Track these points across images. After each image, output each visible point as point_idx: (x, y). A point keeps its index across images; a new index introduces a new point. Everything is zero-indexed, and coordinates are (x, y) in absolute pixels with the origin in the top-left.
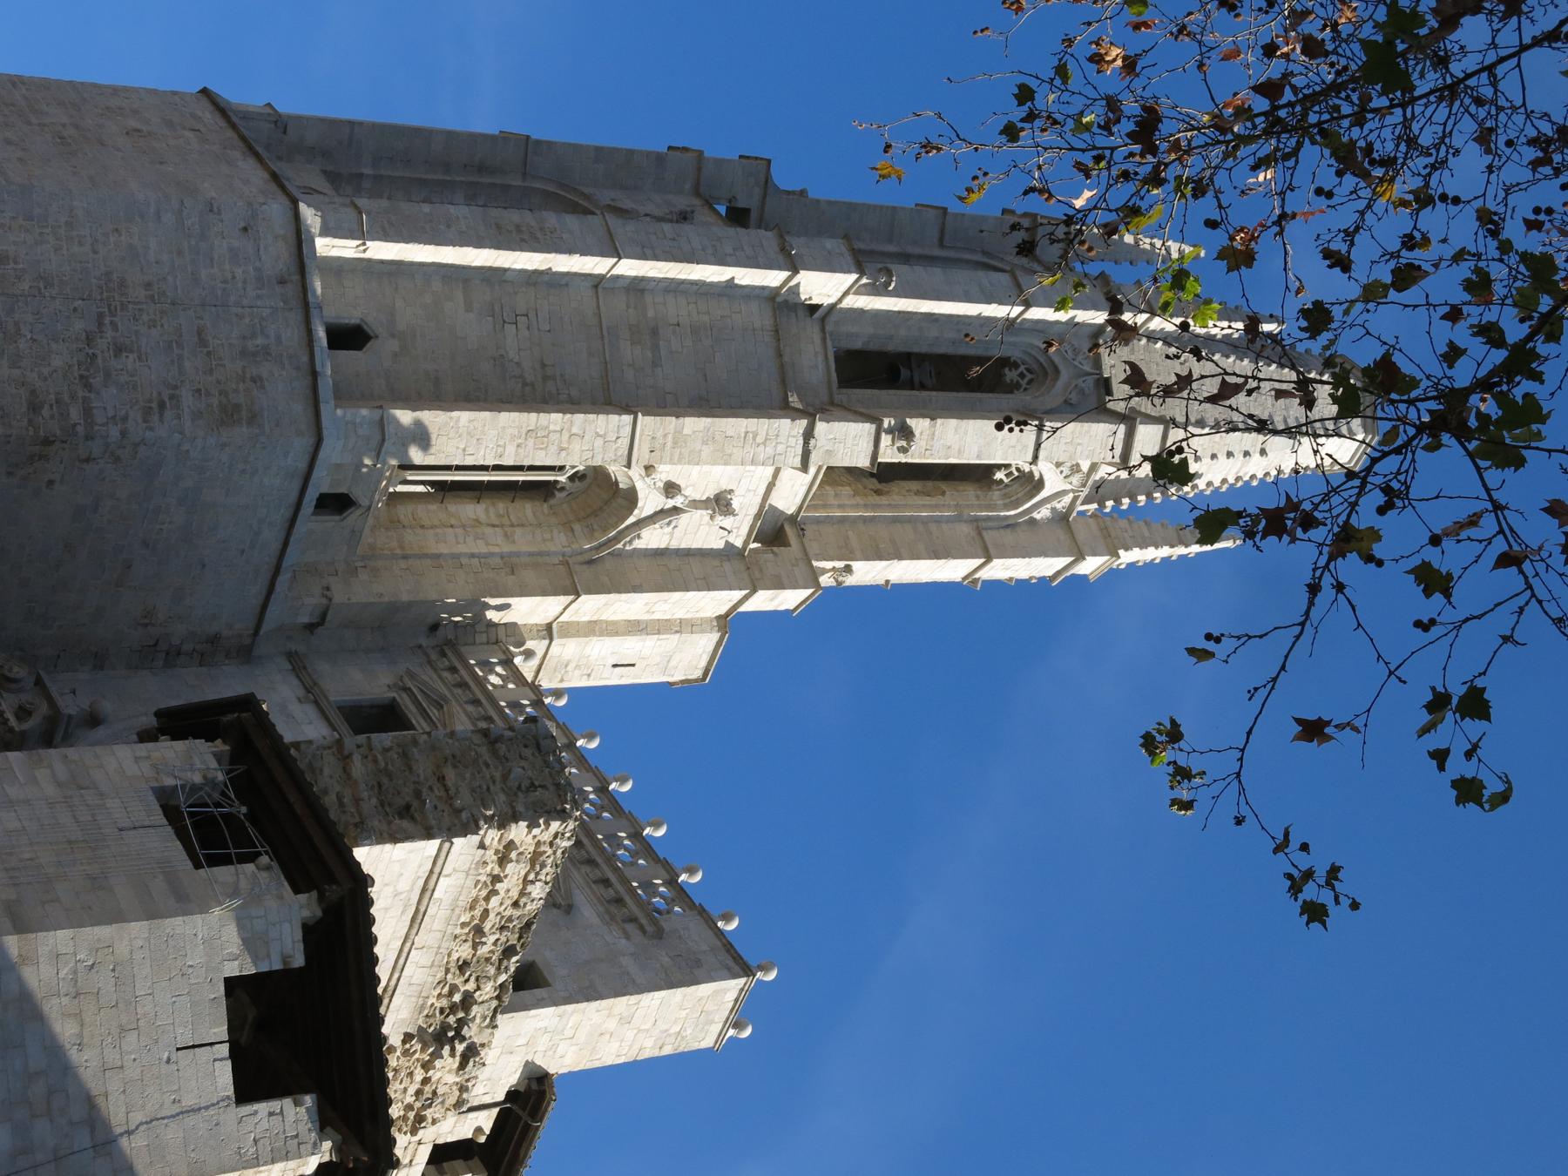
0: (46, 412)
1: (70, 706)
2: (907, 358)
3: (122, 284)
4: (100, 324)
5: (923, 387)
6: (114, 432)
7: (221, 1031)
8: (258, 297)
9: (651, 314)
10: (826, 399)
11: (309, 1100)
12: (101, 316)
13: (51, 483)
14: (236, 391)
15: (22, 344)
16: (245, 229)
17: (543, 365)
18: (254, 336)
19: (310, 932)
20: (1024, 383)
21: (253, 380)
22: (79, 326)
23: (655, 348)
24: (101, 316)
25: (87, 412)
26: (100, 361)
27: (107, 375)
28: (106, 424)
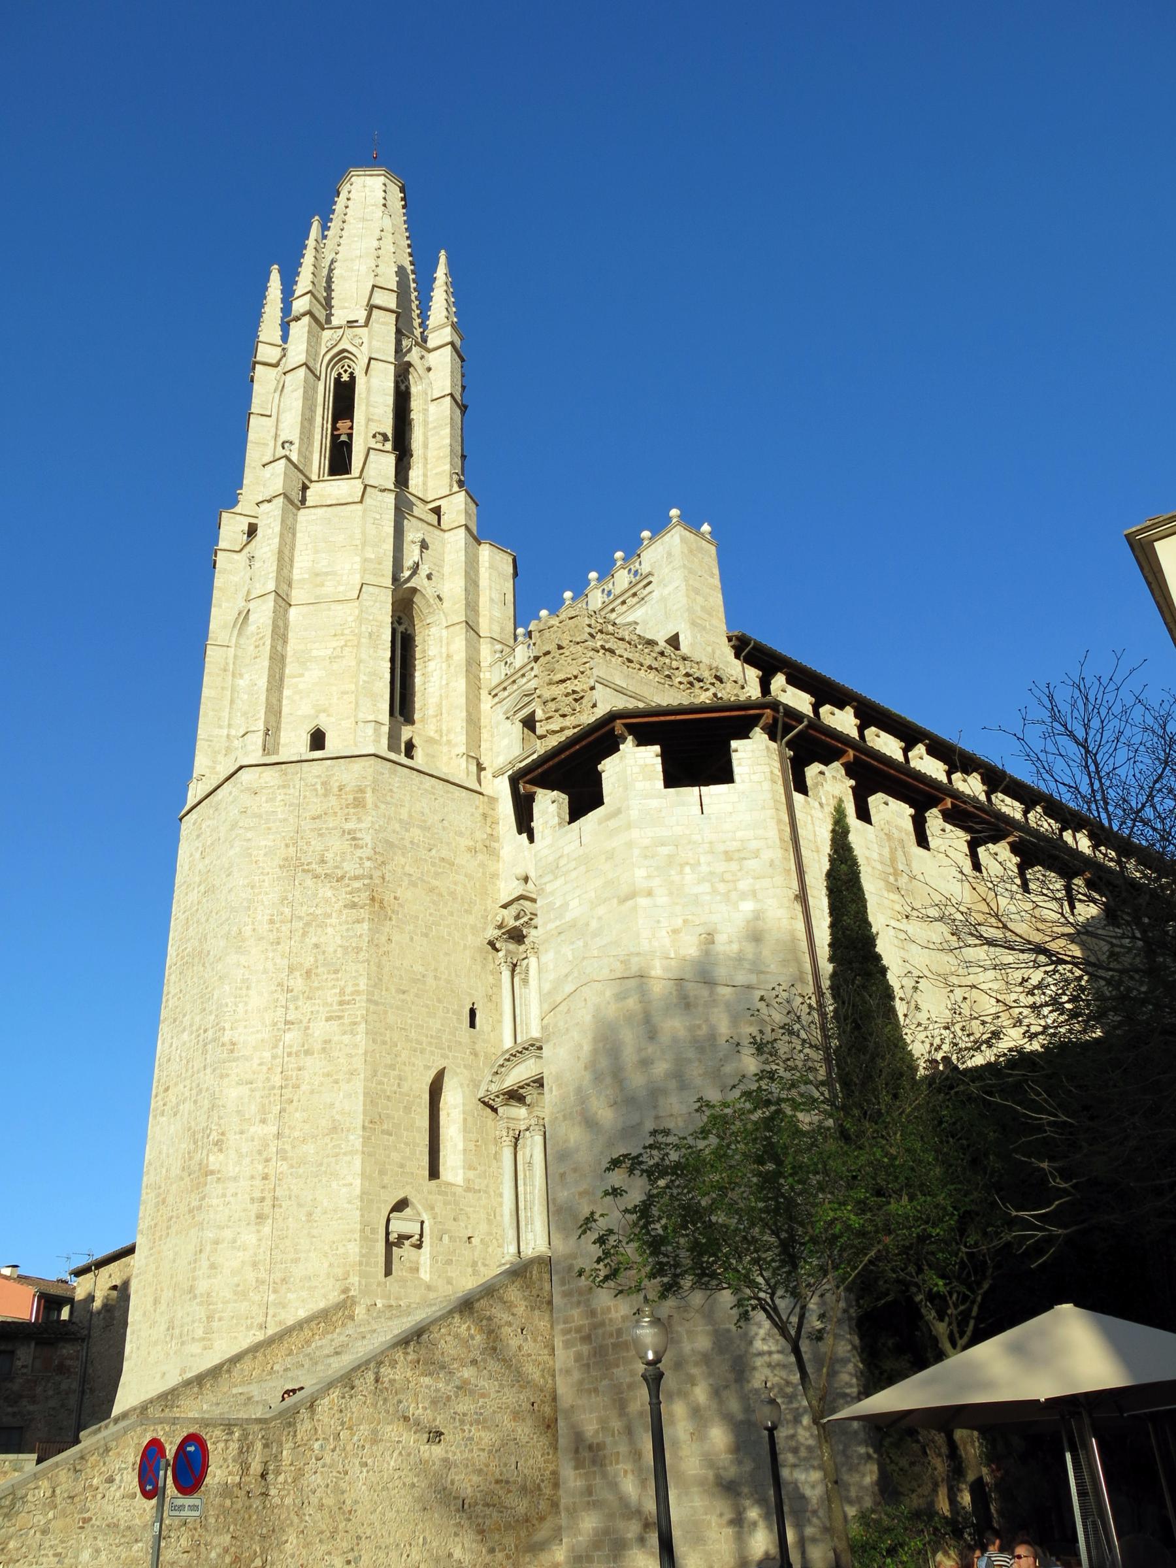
1: (518, 889)
2: (335, 438)
3: (286, 859)
4: (308, 871)
5: (351, 428)
6: (368, 864)
7: (697, 788)
9: (307, 576)
11: (734, 744)
12: (303, 871)
13: (395, 898)
15: (319, 911)
18: (316, 790)
19: (642, 741)
22: (309, 882)
23: (327, 574)
24: (303, 871)
25: (356, 878)
27: (337, 867)
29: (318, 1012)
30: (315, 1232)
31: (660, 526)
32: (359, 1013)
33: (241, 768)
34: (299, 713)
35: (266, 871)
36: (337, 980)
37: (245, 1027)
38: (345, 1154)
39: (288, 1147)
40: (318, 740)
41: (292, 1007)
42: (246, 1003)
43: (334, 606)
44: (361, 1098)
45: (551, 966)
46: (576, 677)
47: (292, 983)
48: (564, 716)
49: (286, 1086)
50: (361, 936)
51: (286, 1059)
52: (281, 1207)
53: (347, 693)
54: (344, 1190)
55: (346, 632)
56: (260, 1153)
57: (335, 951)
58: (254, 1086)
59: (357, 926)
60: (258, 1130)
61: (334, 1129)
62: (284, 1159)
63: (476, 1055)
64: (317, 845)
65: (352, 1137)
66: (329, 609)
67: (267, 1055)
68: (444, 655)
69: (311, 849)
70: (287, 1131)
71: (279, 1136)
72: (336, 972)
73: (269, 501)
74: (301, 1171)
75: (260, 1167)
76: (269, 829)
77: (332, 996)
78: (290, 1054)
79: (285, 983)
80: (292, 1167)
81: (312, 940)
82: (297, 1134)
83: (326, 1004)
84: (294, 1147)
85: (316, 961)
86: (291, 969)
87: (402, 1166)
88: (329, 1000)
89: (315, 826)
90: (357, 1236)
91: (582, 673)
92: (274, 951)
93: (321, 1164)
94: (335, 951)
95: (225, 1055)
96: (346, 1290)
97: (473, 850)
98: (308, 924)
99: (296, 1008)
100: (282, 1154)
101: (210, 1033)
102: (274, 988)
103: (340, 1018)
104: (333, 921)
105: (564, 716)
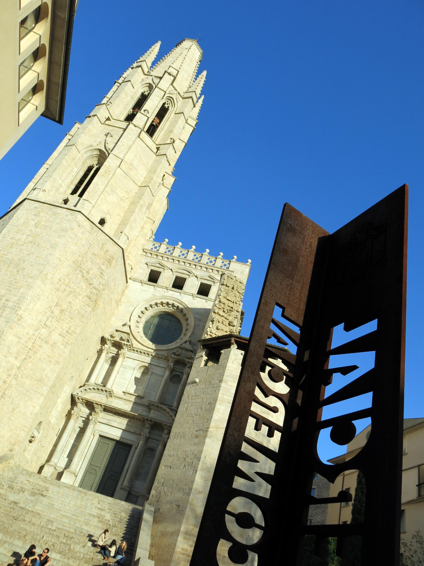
0: (91, 297)
4: (82, 272)
5: (159, 123)
6: (102, 287)
8: (93, 236)
10: (155, 145)
12: (80, 270)
14: (107, 257)
15: (77, 290)
17: (126, 192)
18: (99, 244)
20: (168, 105)
21: (106, 252)
22: (80, 276)
23: (135, 168)
24: (80, 270)
25: (95, 288)
26: (88, 278)
27: (91, 279)
29: (58, 329)
31: (242, 260)
32: (71, 340)
33: (80, 212)
35: (68, 259)
36: (70, 322)
37: (29, 314)
38: (39, 393)
39: (20, 376)
40: (102, 222)
41: (50, 319)
42: (34, 305)
43: (131, 181)
44: (56, 375)
45: (221, 412)
46: (233, 303)
47: (55, 310)
48: (224, 312)
49: (32, 350)
50: (86, 311)
51: (37, 339)
52: (4, 399)
53: (120, 216)
54: (31, 408)
55: (130, 194)
56: (8, 370)
57: (75, 310)
58: (20, 341)
59: (87, 307)
60: (12, 359)
61: (40, 380)
62: (16, 379)
63: (79, 376)
66: (129, 181)
67: (31, 332)
68: (142, 226)
70: (23, 369)
71: (19, 368)
73: (135, 126)
74: (20, 389)
75: (5, 376)
76: (77, 244)
78: (40, 338)
79: (53, 308)
80: (17, 384)
82: (26, 372)
84: (22, 377)
85: (67, 309)
86: (57, 305)
87: (48, 408)
88: (64, 327)
90: (27, 430)
91: (236, 303)
92: (55, 292)
93: (28, 391)
94: (75, 310)
95: (16, 319)
96: (11, 450)
97: (116, 300)
98: (71, 292)
99: (51, 321)
100: (16, 377)
101: (10, 304)
103: (64, 337)
104: (80, 298)
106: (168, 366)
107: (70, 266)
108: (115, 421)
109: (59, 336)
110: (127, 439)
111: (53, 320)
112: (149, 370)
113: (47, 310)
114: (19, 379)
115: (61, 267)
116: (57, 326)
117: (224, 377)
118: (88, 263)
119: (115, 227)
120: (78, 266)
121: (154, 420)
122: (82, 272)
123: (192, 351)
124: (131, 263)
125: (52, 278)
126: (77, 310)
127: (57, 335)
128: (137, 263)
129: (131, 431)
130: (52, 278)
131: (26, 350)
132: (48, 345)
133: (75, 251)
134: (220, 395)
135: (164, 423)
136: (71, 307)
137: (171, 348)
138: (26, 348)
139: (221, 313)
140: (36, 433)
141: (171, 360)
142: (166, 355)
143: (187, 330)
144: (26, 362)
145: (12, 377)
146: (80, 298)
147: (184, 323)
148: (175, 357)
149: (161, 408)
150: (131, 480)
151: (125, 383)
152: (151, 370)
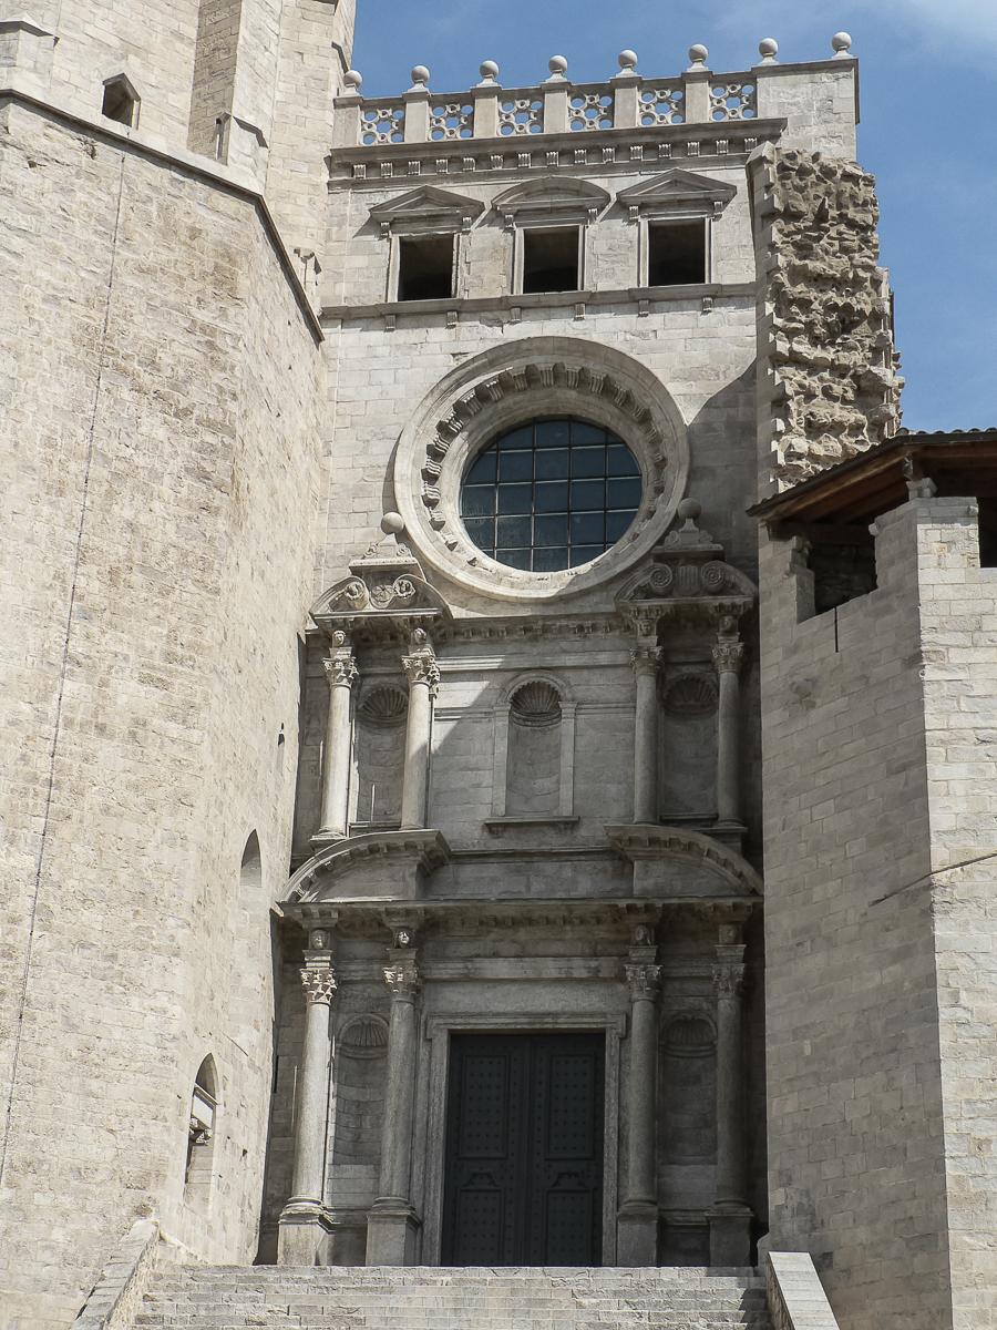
4: (124, 372)
6: (232, 406)
12: (117, 367)
15: (140, 461)
16: (32, 165)
18: (148, 213)
22: (126, 395)
25: (211, 426)
27: (175, 387)
28: (225, 414)
30: (95, 1085)
34: (90, 29)
39: (56, 908)
41: (77, 629)
47: (82, 582)
54: (151, 1018)
57: (165, 553)
64: (144, 329)
65: (171, 922)
69: (133, 329)
72: (165, 593)
74: (76, 958)
76: (56, 251)
77: (154, 639)
78: (69, 723)
79: (70, 581)
80: (60, 946)
81: (124, 511)
82: (71, 884)
83: (140, 648)
88: (149, 644)
89: (140, 286)
92: (51, 503)
93: (113, 957)
94: (165, 553)
97: (303, 438)
102: (48, 580)
103: (163, 685)
105: (816, 341)
106: (637, 654)
107: (67, 360)
108: (496, 955)
109: (144, 688)
110: (574, 1014)
111: (95, 630)
112: (559, 698)
113: (50, 596)
114: (56, 922)
115: (31, 383)
116: (118, 648)
117: (925, 637)
118: (138, 318)
119: (182, 101)
120: (100, 351)
121: (659, 904)
122: (124, 372)
123: (718, 556)
124: (307, 245)
125: (16, 445)
126: (172, 550)
127: (134, 684)
128: (328, 232)
129: (576, 974)
130: (16, 445)
131: (36, 794)
132: (115, 743)
133: (61, 284)
134: (931, 721)
135: (709, 903)
136: (145, 545)
137: (619, 569)
138: (30, 786)
139: (803, 347)
140: (203, 1112)
141: (641, 625)
142: (611, 608)
143: (661, 465)
144: (56, 843)
145: (28, 921)
146: (166, 492)
147: (636, 438)
148: (655, 602)
149: (671, 843)
150: (653, 1172)
151: (478, 786)
152: (566, 693)
